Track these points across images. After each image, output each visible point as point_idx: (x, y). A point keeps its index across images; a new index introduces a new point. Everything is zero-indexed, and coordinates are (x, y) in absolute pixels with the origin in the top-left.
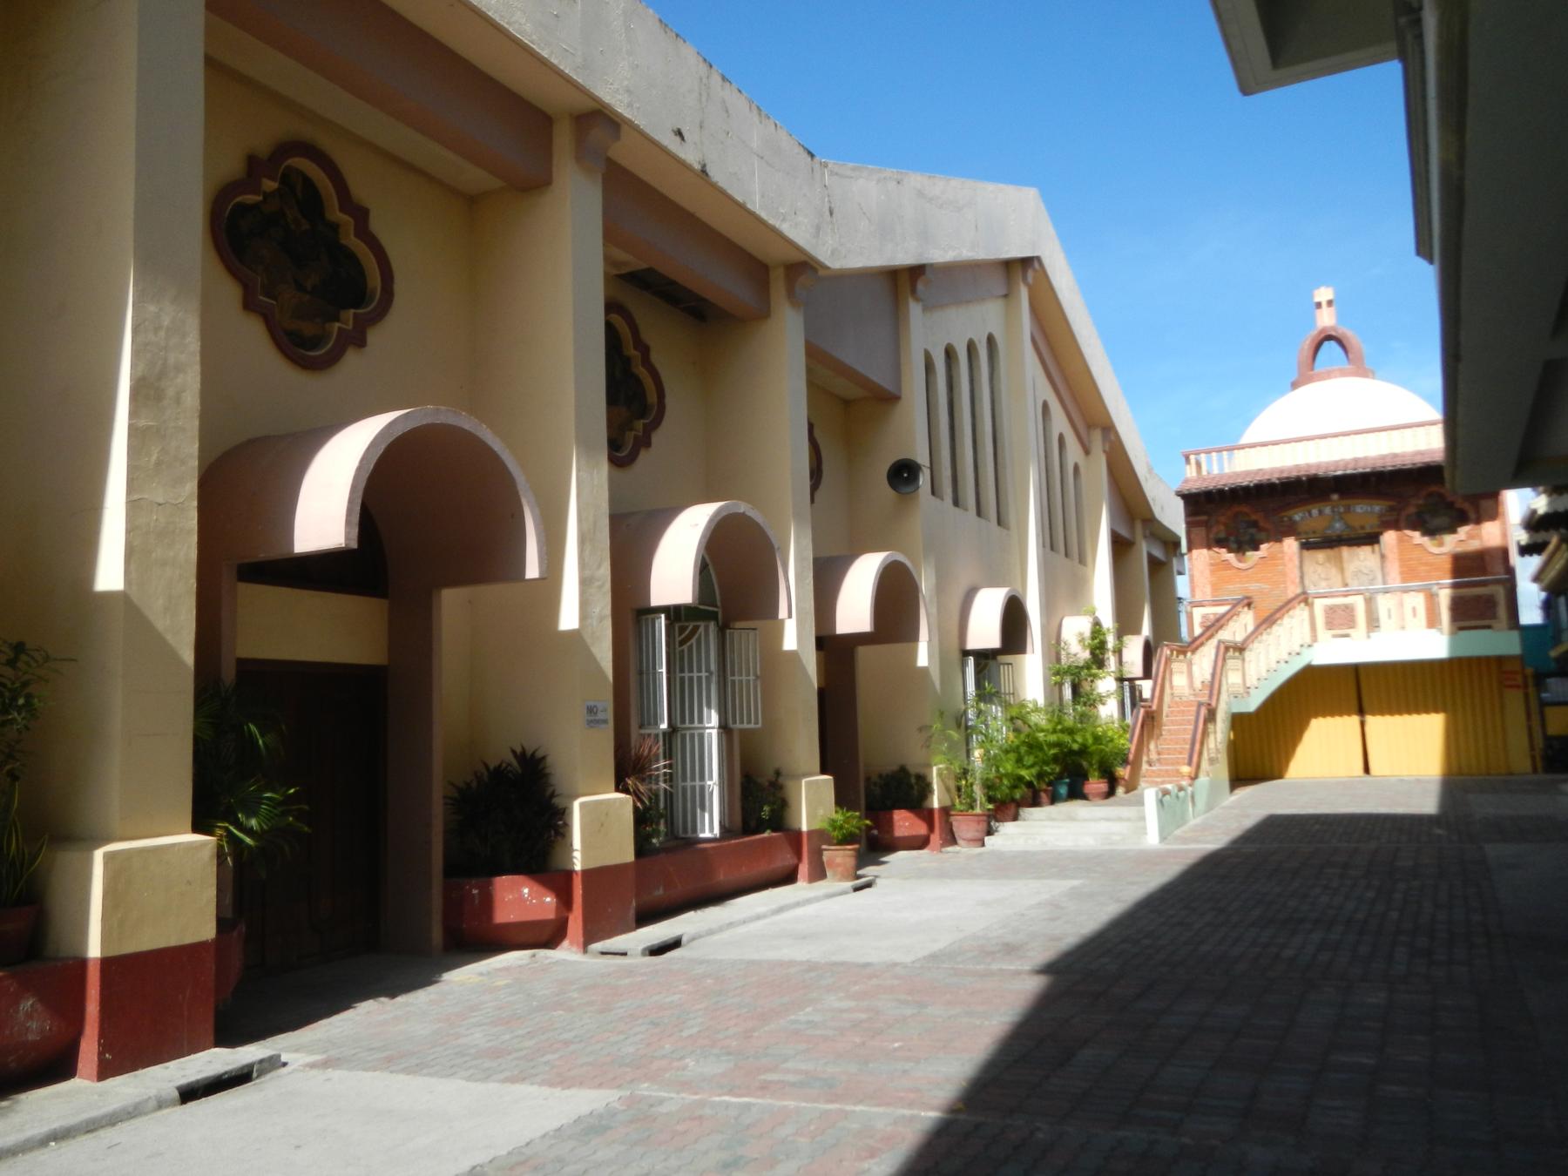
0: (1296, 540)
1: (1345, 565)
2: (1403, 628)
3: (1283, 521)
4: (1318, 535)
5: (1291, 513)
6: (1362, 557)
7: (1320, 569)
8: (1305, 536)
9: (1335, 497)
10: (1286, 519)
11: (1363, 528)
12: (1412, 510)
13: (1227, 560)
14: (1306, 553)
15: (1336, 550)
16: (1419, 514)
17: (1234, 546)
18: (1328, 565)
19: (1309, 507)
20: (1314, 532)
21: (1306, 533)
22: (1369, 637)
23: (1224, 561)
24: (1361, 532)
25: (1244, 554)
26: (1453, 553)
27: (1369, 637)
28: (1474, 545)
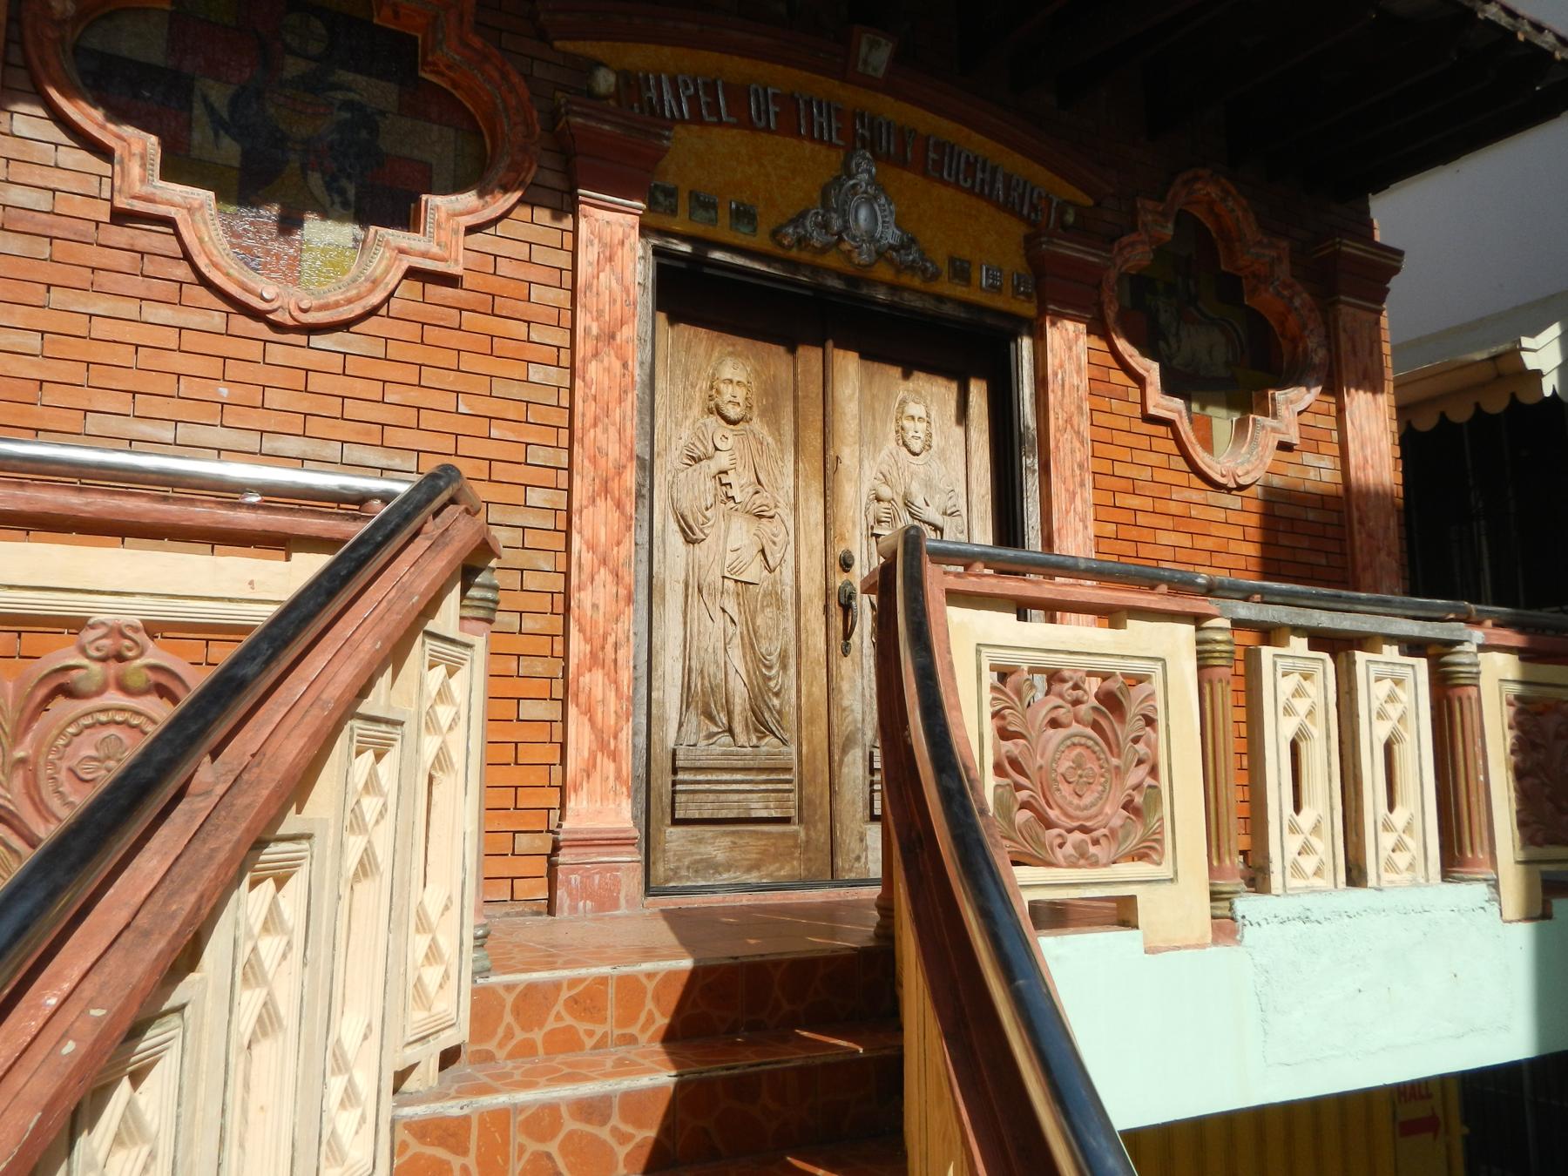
0: (645, 230)
1: (848, 453)
2: (1355, 875)
3: (591, 94)
4: (761, 241)
5: (639, 56)
6: (915, 430)
7: (727, 439)
8: (698, 229)
9: (877, 56)
10: (605, 81)
11: (961, 271)
12: (1137, 255)
13: (169, 222)
14: (662, 317)
15: (810, 356)
16: (1139, 284)
17: (230, 151)
18: (757, 425)
19: (737, 67)
20: (745, 215)
21: (703, 204)
22: (1225, 926)
23: (121, 217)
24: (945, 287)
25: (289, 224)
26: (1268, 489)
27: (1225, 926)
28: (1319, 472)
